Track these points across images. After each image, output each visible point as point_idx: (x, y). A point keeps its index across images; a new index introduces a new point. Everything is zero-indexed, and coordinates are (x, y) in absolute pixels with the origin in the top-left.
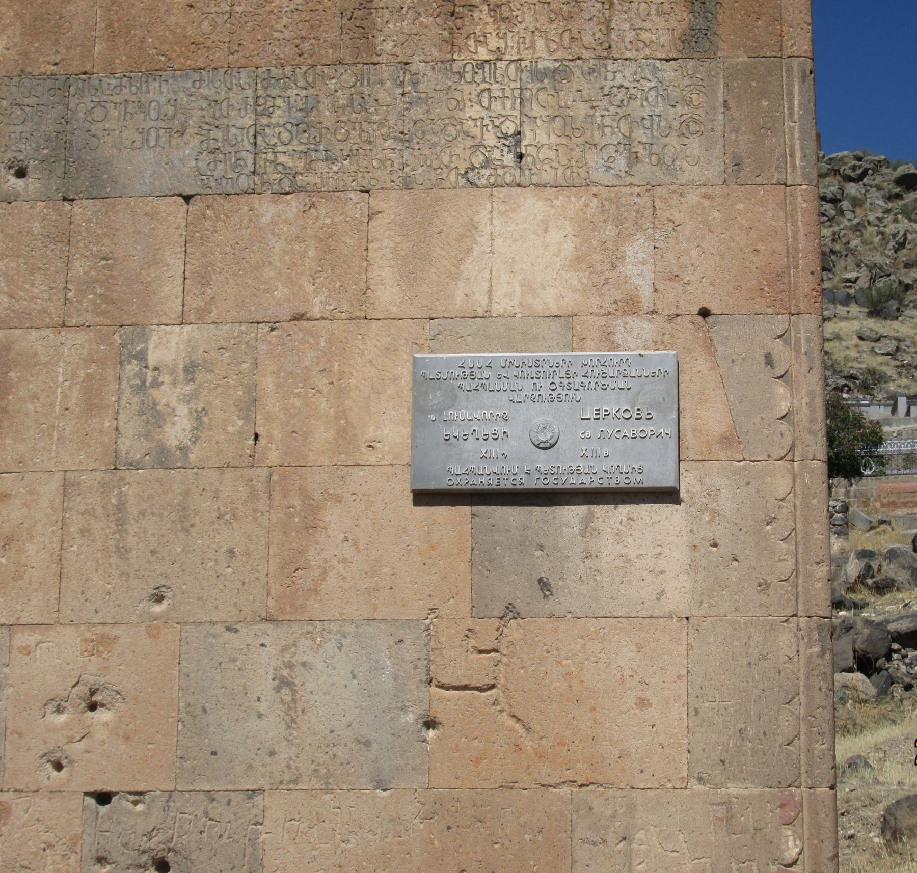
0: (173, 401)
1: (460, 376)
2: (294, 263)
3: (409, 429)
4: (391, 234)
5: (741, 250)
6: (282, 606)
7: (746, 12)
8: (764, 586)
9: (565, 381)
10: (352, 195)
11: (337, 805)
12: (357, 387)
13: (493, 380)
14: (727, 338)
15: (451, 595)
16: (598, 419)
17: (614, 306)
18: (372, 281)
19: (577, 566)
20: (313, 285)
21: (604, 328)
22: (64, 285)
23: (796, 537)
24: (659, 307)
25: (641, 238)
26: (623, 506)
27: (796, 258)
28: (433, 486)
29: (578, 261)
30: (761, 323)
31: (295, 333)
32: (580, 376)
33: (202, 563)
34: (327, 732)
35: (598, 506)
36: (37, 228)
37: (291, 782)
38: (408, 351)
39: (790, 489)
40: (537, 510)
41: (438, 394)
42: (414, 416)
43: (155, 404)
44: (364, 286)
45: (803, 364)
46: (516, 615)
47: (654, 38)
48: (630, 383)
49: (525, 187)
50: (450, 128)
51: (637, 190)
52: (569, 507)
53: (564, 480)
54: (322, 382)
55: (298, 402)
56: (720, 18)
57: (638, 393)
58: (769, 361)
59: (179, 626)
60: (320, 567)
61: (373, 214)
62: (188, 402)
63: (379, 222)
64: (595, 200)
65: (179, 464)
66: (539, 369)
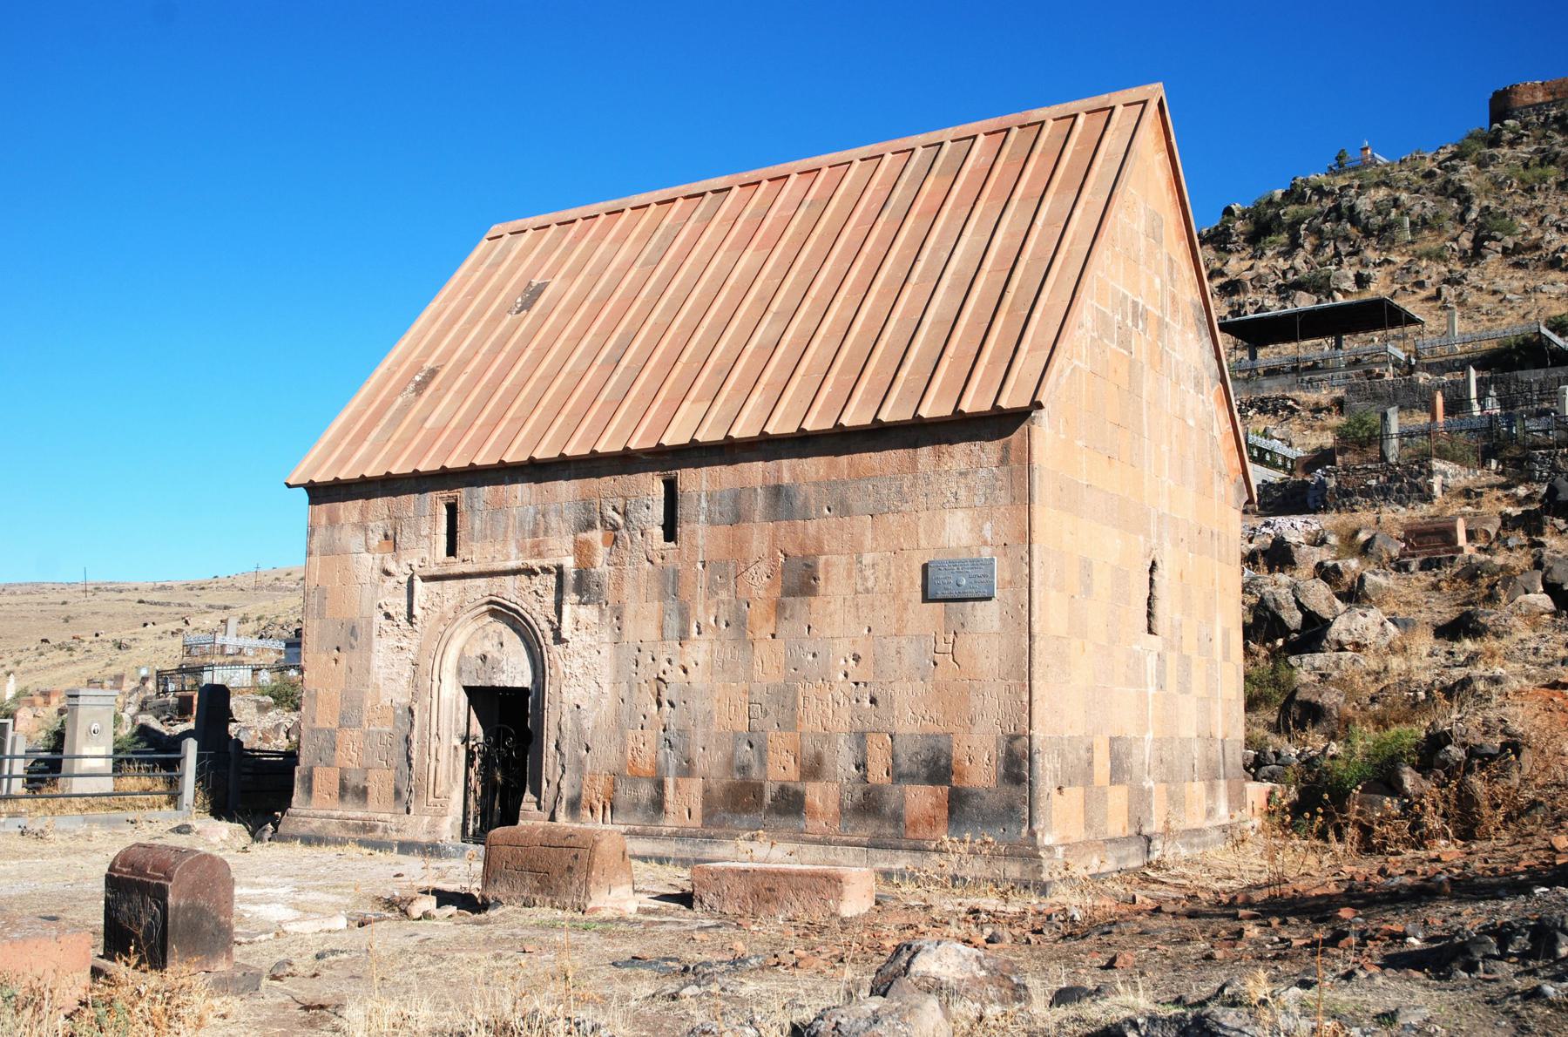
25: (988, 524)
40: (961, 604)
58: (1022, 558)
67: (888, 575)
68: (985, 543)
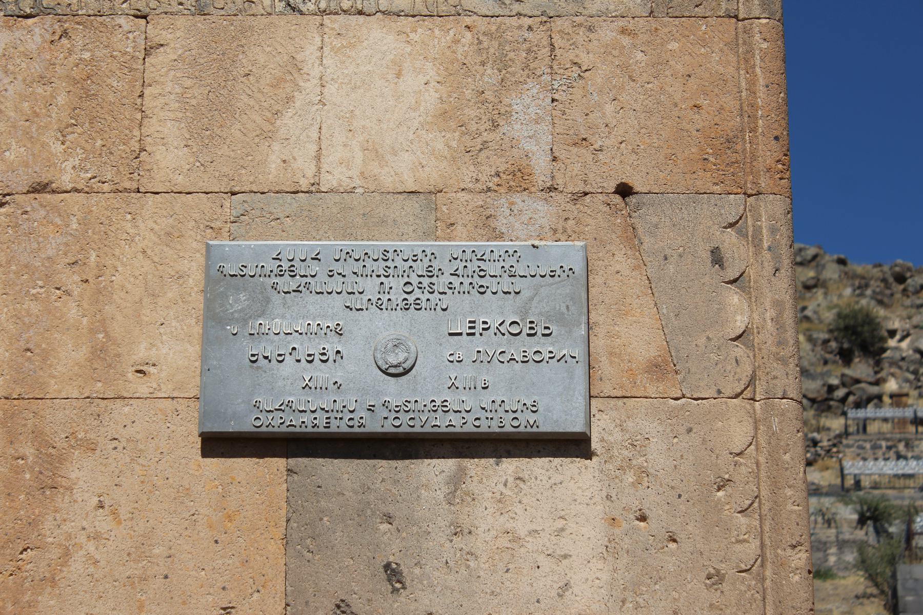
1: (275, 273)
2: (35, 112)
3: (198, 348)
4: (178, 75)
5: (676, 105)
8: (715, 578)
9: (426, 281)
10: (122, 20)
12: (123, 287)
13: (322, 277)
14: (656, 226)
15: (255, 588)
16: (473, 334)
17: (496, 180)
18: (149, 139)
19: (442, 546)
20: (63, 143)
21: (482, 209)
23: (760, 509)
24: (560, 181)
26: (509, 460)
27: (753, 117)
28: (232, 427)
30: (705, 206)
31: (34, 210)
32: (447, 274)
35: (472, 461)
38: (199, 237)
39: (750, 438)
40: (384, 466)
41: (242, 297)
42: (205, 328)
44: (137, 147)
45: (766, 264)
49: (369, 15)
51: (527, 22)
52: (430, 461)
53: (424, 420)
54: (71, 280)
55: (35, 308)
57: (531, 299)
58: (717, 257)
60: (60, 545)
61: (151, 48)
63: (160, 58)
64: (469, 35)
66: (389, 263)
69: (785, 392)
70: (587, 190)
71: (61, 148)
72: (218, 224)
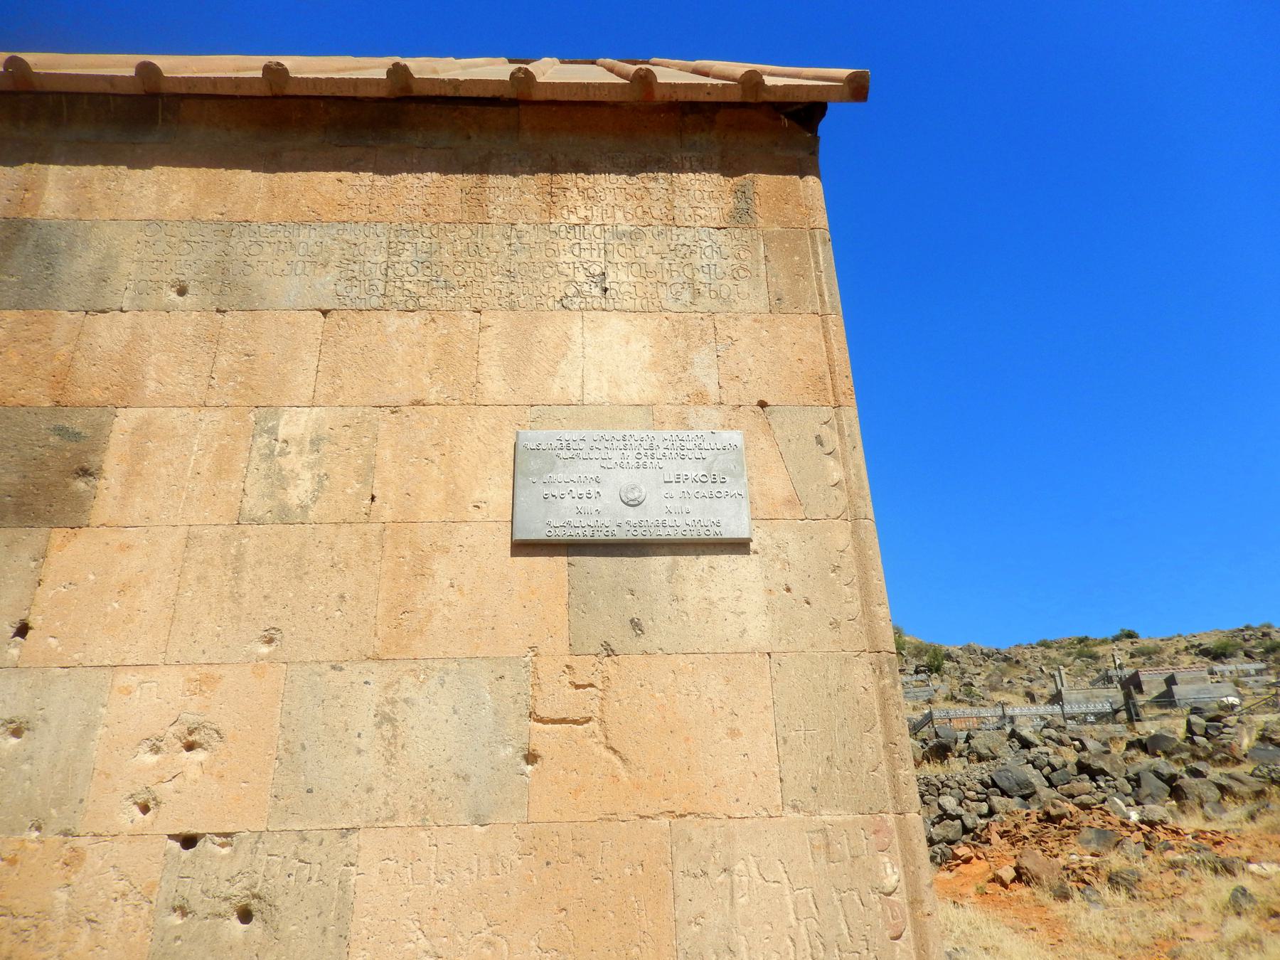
0: (298, 467)
5: (788, 359)
6: (388, 646)
7: (777, 199)
8: (835, 624)
9: (649, 452)
10: (466, 313)
11: (434, 842)
12: (466, 458)
17: (687, 398)
22: (209, 374)
24: (724, 399)
29: (655, 364)
32: (661, 448)
33: (313, 607)
34: (426, 767)
36: (189, 331)
37: (388, 819)
40: (627, 561)
43: (281, 470)
44: (475, 380)
45: (848, 444)
46: (610, 653)
47: (707, 214)
48: (705, 454)
50: (548, 269)
51: (700, 315)
54: (434, 454)
55: (412, 470)
56: (757, 202)
57: (713, 462)
58: (819, 440)
59: (284, 665)
62: (312, 468)
64: (667, 322)
65: (299, 520)
67: (368, 471)
68: (700, 398)
69: (866, 515)
70: (740, 404)
71: (429, 381)
72: (524, 422)
